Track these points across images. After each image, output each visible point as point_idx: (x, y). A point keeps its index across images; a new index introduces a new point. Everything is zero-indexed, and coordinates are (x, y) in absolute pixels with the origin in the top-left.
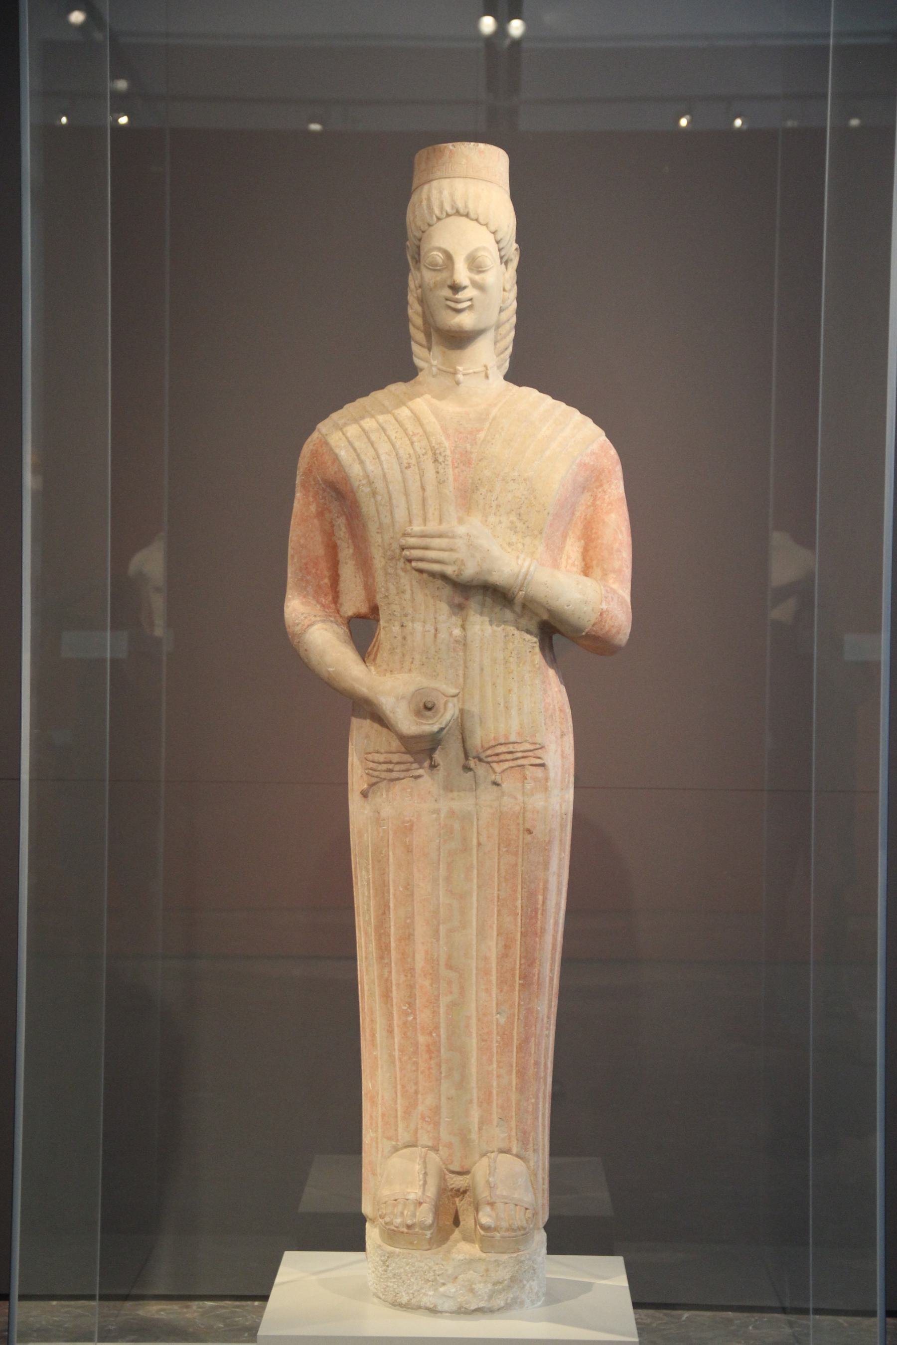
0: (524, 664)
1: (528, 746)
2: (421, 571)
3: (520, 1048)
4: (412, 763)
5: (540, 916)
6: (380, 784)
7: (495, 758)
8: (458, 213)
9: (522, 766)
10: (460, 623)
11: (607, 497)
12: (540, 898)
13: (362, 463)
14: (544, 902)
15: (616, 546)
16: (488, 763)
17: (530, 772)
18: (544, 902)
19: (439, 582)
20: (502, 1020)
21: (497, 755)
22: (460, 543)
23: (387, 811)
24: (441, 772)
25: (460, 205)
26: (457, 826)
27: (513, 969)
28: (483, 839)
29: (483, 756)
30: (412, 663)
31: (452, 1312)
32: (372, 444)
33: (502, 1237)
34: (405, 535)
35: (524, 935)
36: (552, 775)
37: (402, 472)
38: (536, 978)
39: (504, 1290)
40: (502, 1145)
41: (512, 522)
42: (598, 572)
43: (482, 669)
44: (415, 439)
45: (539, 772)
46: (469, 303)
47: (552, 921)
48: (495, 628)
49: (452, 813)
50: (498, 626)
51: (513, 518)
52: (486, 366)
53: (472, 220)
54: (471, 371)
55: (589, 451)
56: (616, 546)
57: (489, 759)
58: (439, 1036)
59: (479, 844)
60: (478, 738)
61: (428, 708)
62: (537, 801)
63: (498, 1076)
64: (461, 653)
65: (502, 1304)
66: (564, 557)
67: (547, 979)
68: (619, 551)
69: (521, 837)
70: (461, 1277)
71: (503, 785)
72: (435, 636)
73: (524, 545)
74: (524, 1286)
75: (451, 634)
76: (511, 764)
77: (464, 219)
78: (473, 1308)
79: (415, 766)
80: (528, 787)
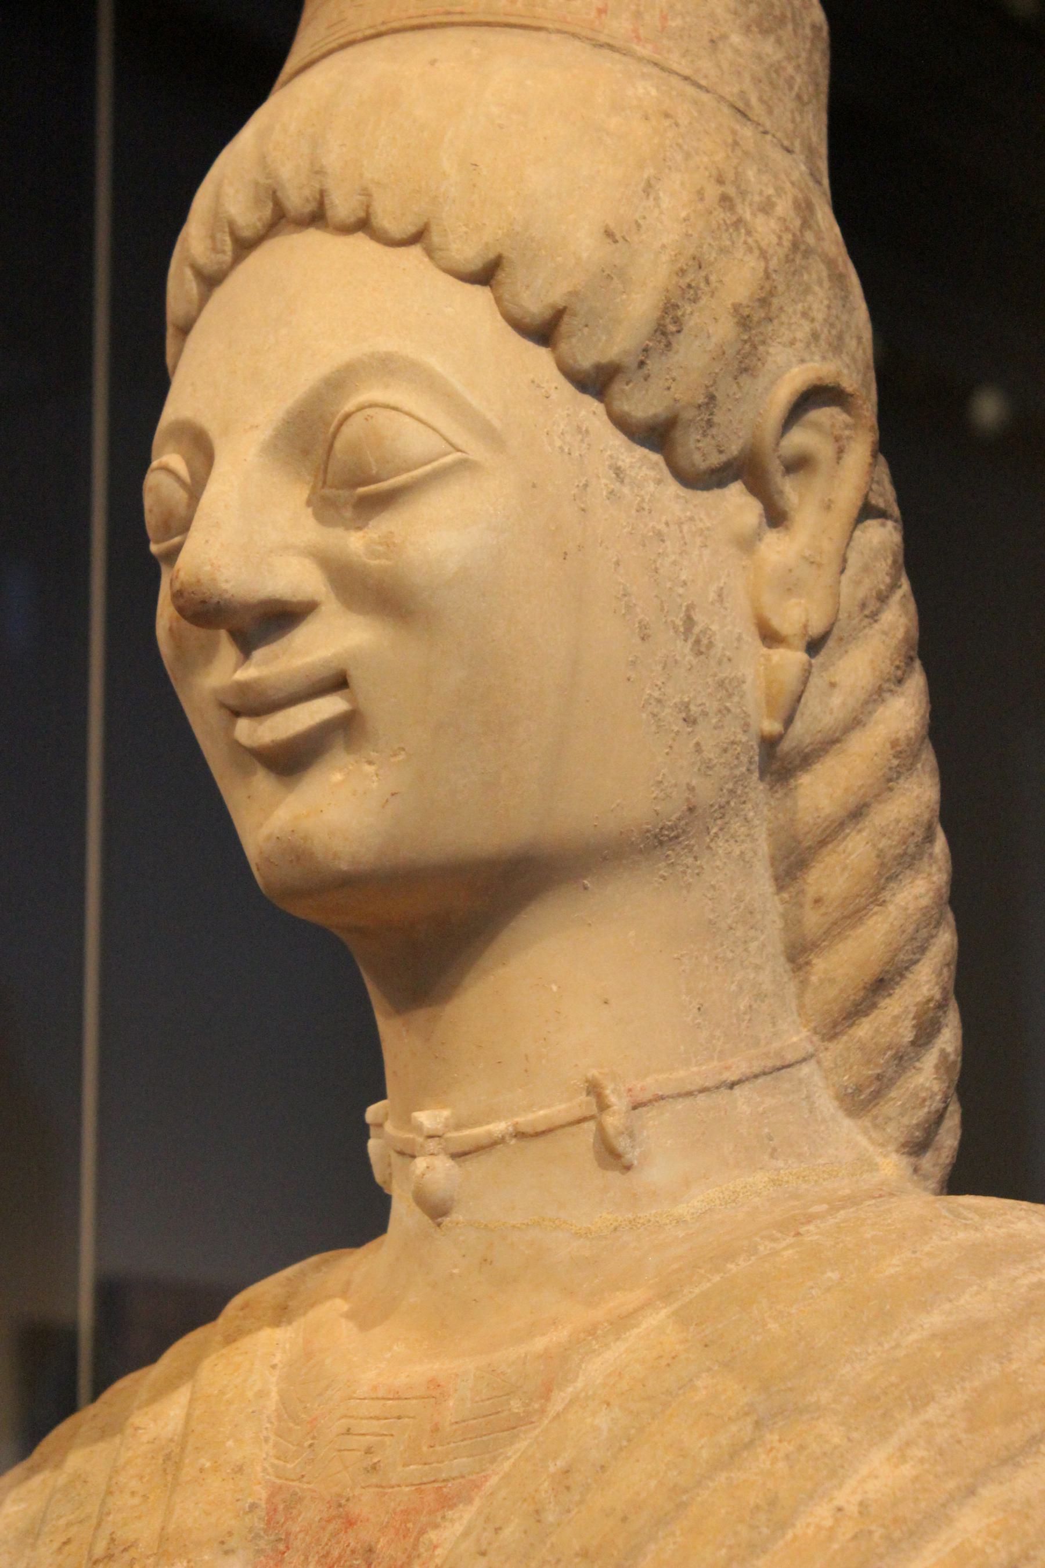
46: (330, 706)
52: (594, 1089)
53: (346, 229)
54: (499, 1127)
77: (313, 237)
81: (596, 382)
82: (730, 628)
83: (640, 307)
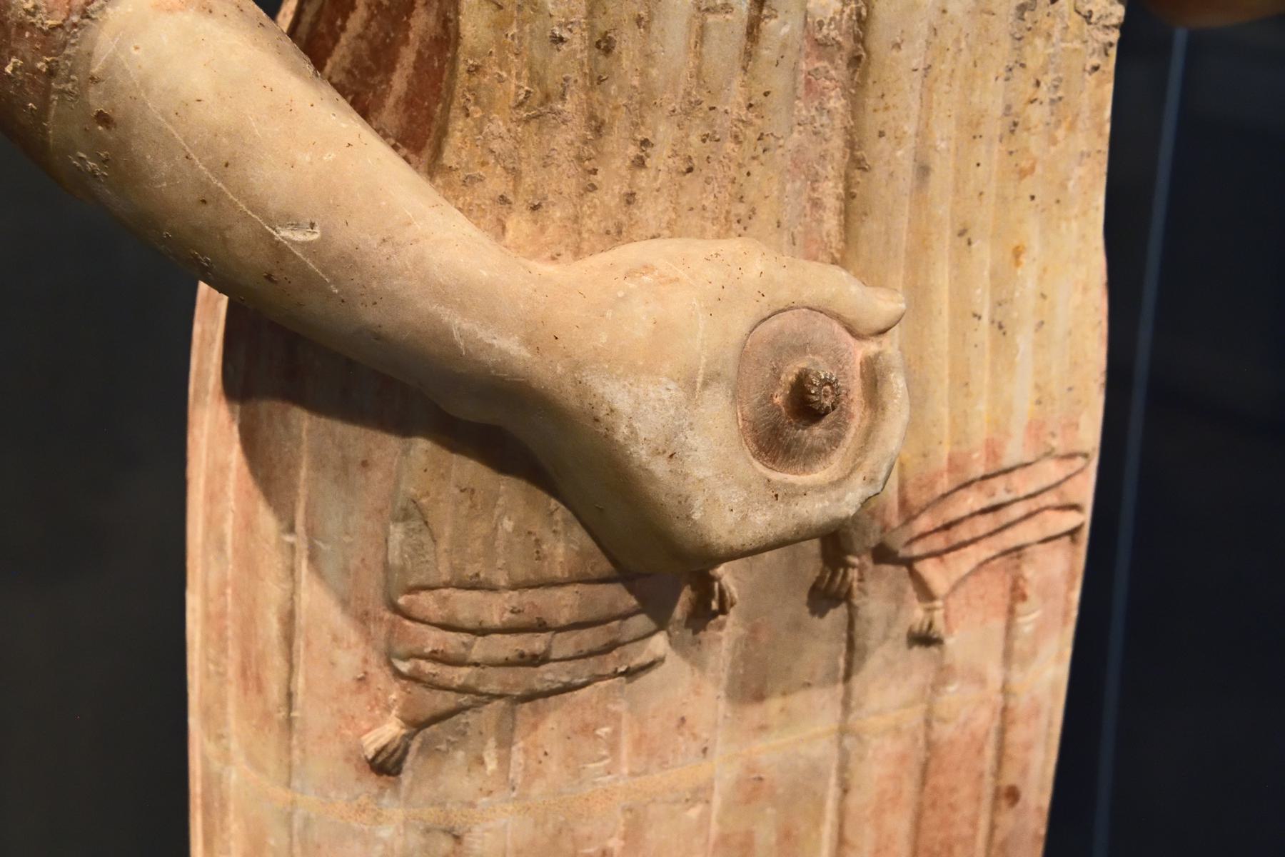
0: (1072, 127)
4: (625, 616)
6: (470, 717)
7: (938, 542)
9: (1017, 551)
16: (909, 563)
24: (726, 636)
30: (640, 163)
43: (924, 171)
49: (753, 787)
57: (917, 549)
64: (836, 103)
69: (983, 824)
71: (950, 642)
72: (753, 30)
79: (641, 622)
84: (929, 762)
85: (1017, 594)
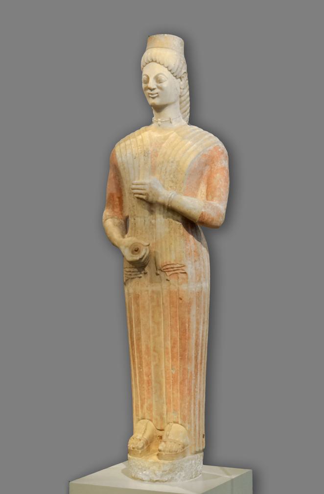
1: (179, 266)
2: (138, 198)
3: (181, 383)
5: (187, 332)
7: (167, 270)
8: (152, 61)
9: (177, 273)
10: (154, 217)
11: (216, 167)
12: (187, 325)
13: (121, 157)
14: (189, 325)
15: (218, 186)
16: (165, 272)
17: (181, 276)
18: (189, 325)
19: (144, 202)
20: (174, 372)
21: (167, 269)
22: (146, 187)
23: (131, 291)
24: (148, 276)
25: (154, 58)
26: (155, 297)
27: (177, 353)
28: (164, 302)
29: (162, 269)
31: (149, 481)
32: (126, 149)
33: (166, 454)
34: (133, 184)
35: (180, 339)
36: (190, 276)
37: (133, 160)
38: (187, 356)
39: (167, 474)
40: (175, 420)
41: (171, 178)
42: (210, 197)
44: (139, 147)
45: (184, 275)
46: (157, 95)
47: (194, 334)
48: (165, 219)
49: (153, 292)
50: (166, 218)
51: (172, 176)
52: (170, 118)
55: (208, 149)
56: (218, 186)
57: (165, 270)
58: (151, 377)
59: (163, 304)
60: (161, 262)
61: (136, 250)
62: (184, 287)
63: (173, 394)
65: (167, 480)
66: (199, 192)
67: (193, 357)
68: (219, 188)
70: (151, 468)
73: (176, 187)
74: (176, 474)
75: (151, 222)
76: (173, 272)
77: (155, 63)
78: (155, 480)
79: (139, 273)
80: (180, 281)
81: (173, 74)
82: (179, 89)
83: (176, 69)
84: (170, 292)
85: (178, 278)
